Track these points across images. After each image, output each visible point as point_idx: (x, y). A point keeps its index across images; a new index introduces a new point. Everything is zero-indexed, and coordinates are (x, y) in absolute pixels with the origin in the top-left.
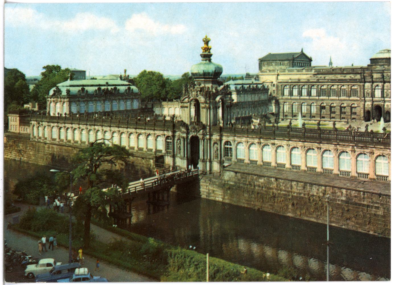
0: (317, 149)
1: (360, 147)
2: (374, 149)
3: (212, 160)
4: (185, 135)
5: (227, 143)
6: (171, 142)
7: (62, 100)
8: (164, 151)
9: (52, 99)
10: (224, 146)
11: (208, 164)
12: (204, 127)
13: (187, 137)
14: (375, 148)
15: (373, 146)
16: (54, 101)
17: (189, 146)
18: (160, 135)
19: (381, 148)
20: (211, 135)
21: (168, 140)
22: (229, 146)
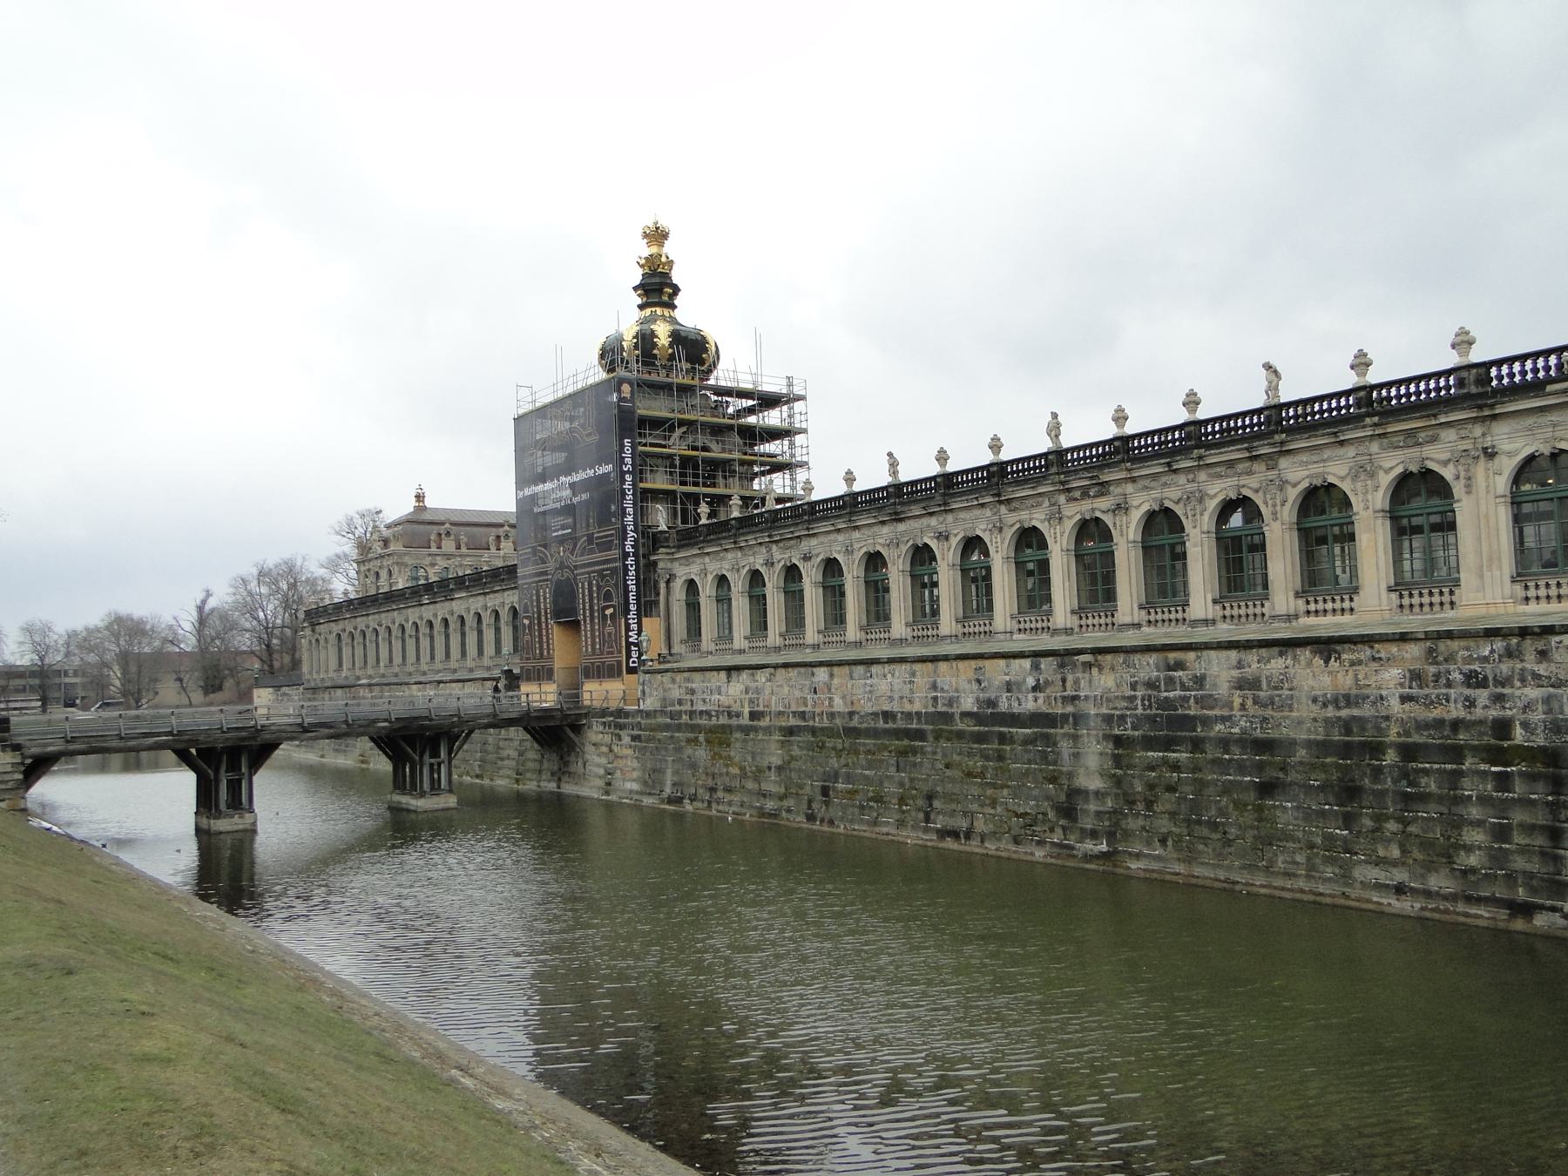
0: (935, 541)
1: (1077, 494)
2: (1129, 488)
14: (1133, 480)
15: (1123, 475)
19: (1155, 476)
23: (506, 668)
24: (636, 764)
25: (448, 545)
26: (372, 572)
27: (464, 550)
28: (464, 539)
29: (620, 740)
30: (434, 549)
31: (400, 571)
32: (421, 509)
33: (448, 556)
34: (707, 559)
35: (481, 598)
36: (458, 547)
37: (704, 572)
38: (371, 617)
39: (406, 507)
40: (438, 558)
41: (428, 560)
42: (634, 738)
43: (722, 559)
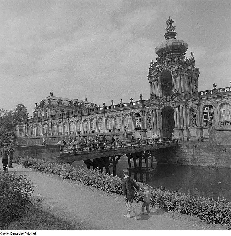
3: (189, 128)
4: (156, 107)
5: (205, 108)
6: (139, 119)
7: (46, 109)
8: (132, 129)
9: (39, 109)
10: (203, 111)
11: (185, 132)
12: (179, 95)
13: (159, 109)
16: (40, 110)
17: (161, 117)
18: (128, 114)
20: (186, 102)
21: (135, 118)
22: (209, 111)
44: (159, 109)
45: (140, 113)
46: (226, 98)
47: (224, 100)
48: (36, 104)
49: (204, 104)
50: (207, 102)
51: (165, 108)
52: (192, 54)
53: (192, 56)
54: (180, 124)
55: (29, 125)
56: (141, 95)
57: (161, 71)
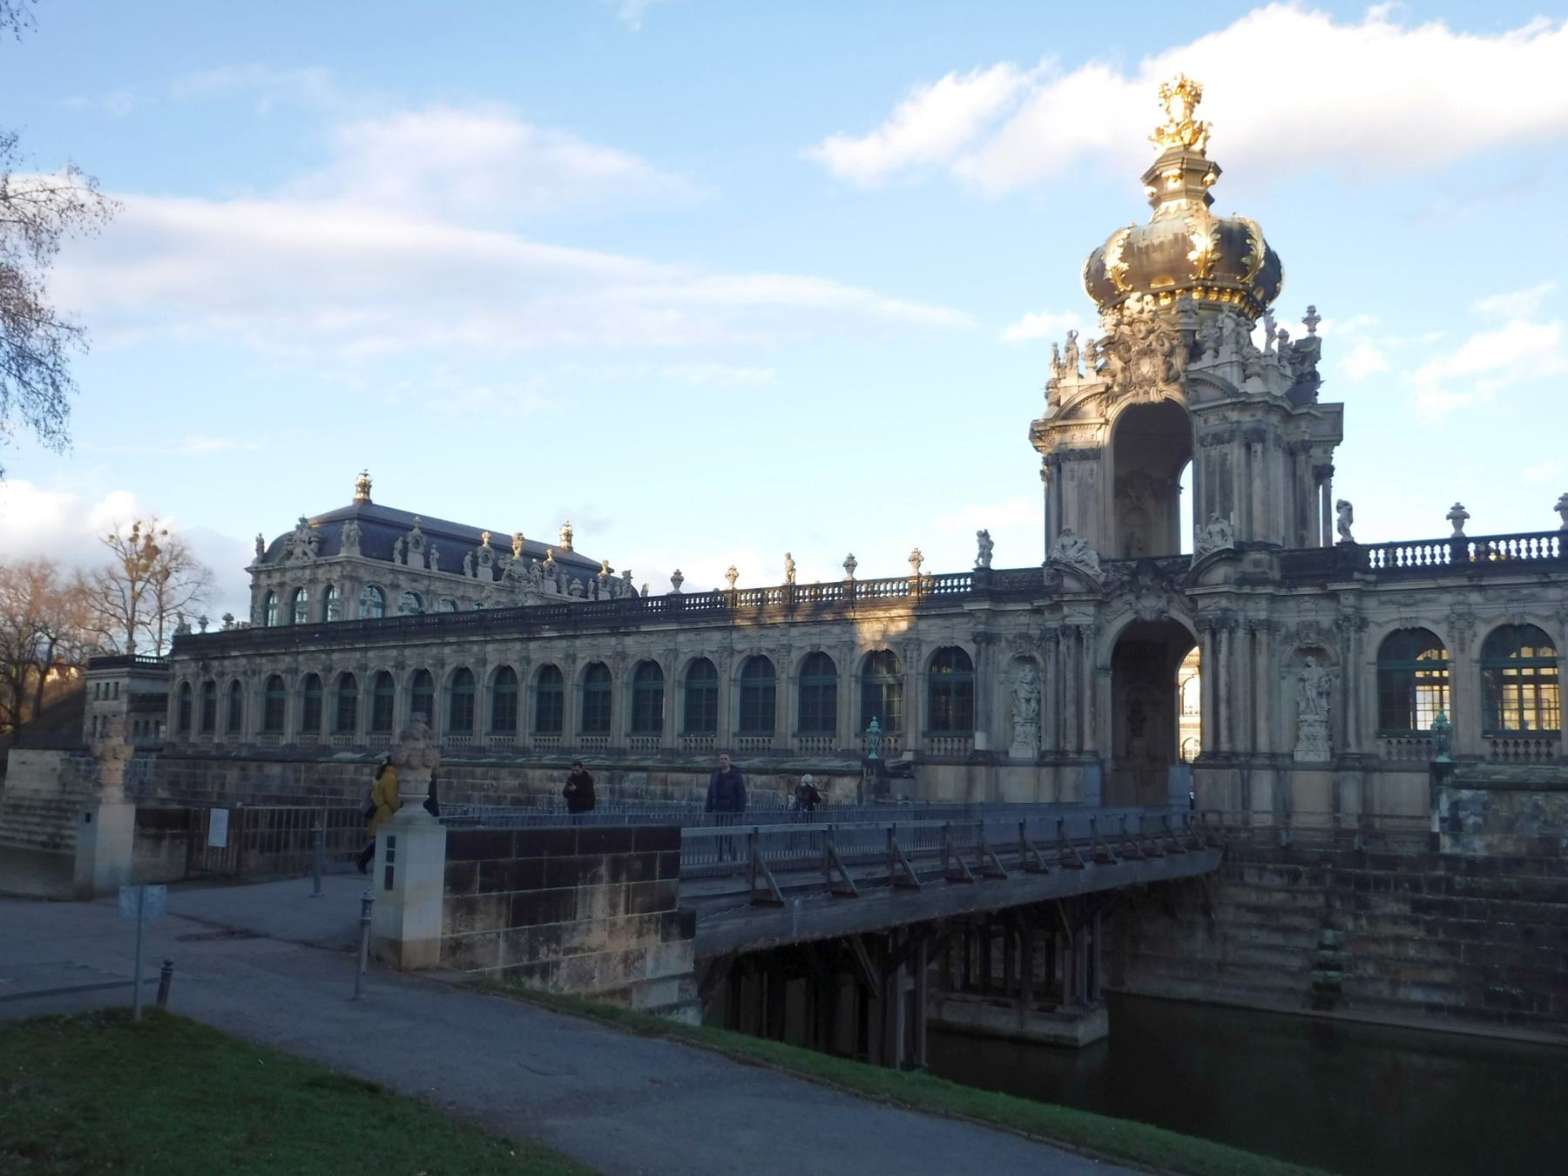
16: (282, 585)
17: (1106, 682)
23: (873, 756)
24: (1436, 955)
25: (416, 561)
26: (288, 588)
27: (434, 568)
28: (435, 554)
29: (1363, 904)
30: (398, 562)
31: (353, 591)
32: (366, 502)
33: (414, 577)
34: (1475, 597)
35: (717, 636)
36: (427, 566)
37: (1462, 620)
38: (371, 654)
39: (343, 498)
40: (401, 577)
41: (388, 579)
42: (1418, 906)
43: (1532, 598)
44: (1098, 631)
45: (970, 649)
46: (1525, 599)
47: (1515, 608)
48: (261, 542)
49: (1385, 618)
50: (1407, 612)
51: (1136, 626)
52: (1312, 319)
53: (1312, 330)
54: (1231, 738)
55: (206, 669)
56: (984, 536)
57: (1124, 402)
